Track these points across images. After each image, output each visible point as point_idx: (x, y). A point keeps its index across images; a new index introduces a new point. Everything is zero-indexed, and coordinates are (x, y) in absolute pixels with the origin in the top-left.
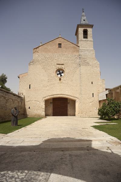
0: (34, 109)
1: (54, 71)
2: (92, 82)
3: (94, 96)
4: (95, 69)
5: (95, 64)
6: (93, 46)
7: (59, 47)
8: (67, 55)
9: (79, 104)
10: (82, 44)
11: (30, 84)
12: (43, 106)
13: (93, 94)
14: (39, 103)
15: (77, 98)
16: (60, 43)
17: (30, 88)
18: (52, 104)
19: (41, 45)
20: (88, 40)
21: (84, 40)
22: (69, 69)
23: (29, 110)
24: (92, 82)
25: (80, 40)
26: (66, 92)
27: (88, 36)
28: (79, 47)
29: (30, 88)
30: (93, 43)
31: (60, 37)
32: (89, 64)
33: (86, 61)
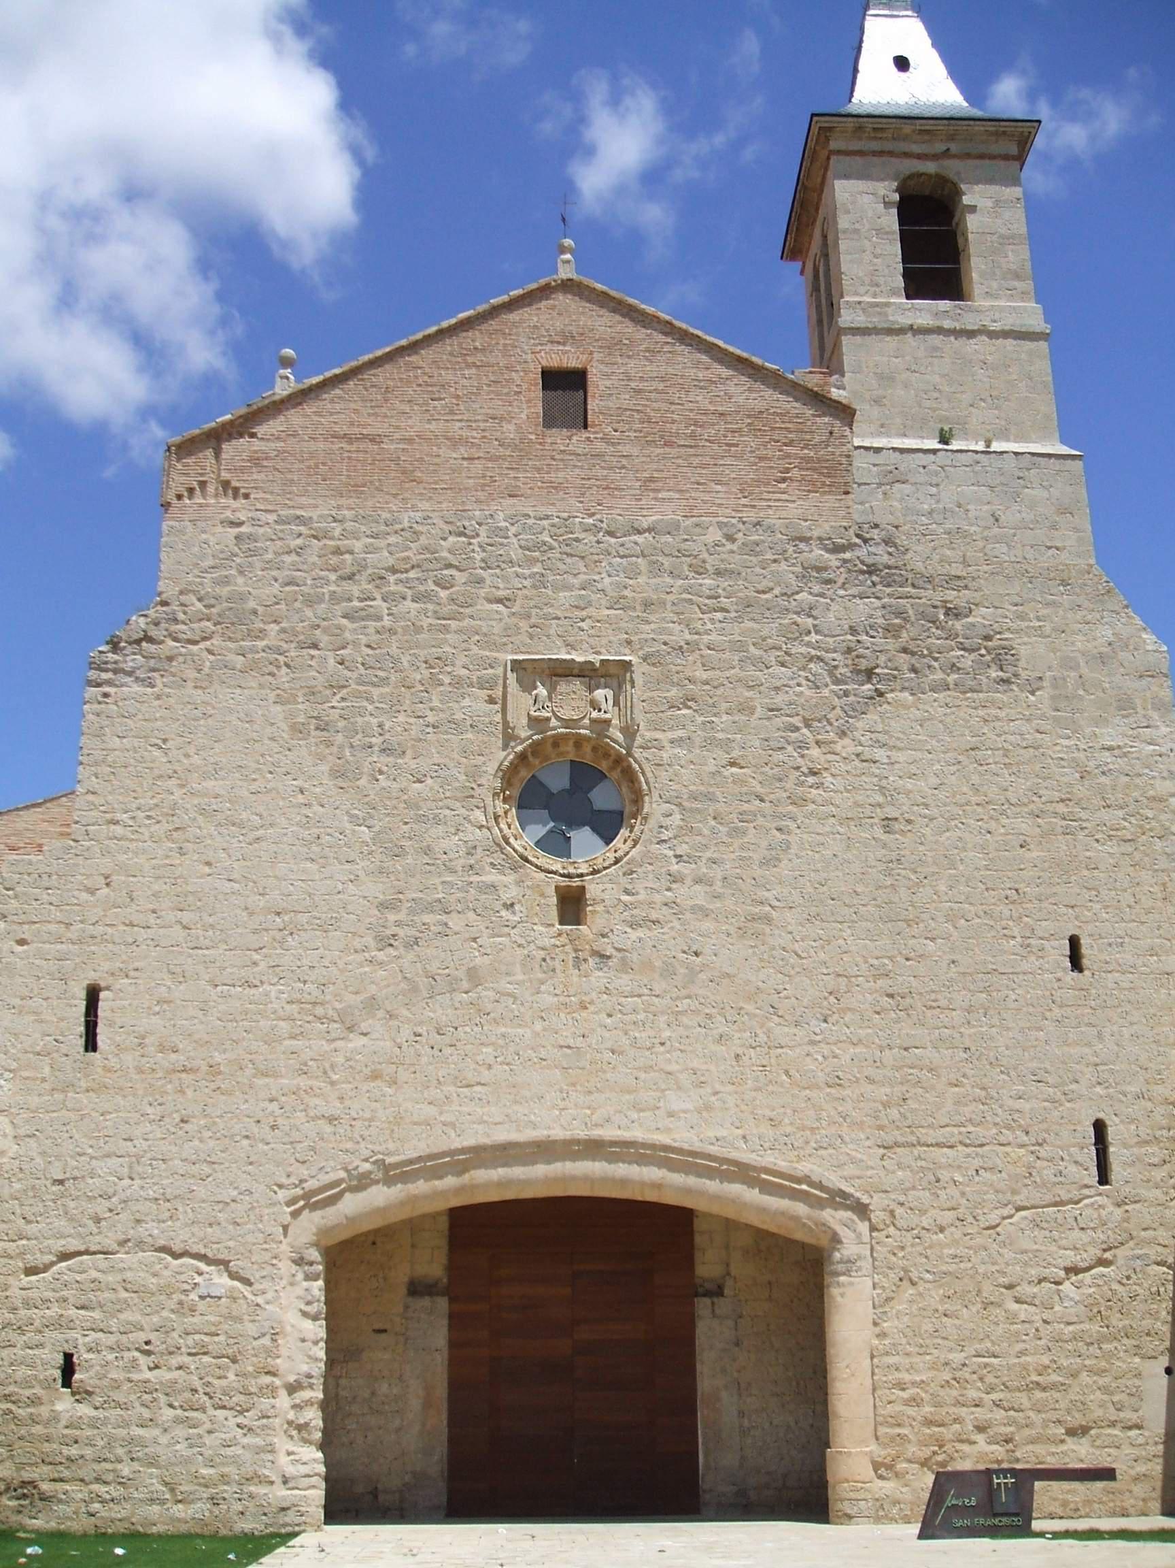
0: (146, 1388)
1: (474, 774)
2: (1074, 942)
3: (1117, 1170)
4: (1110, 735)
5: (1102, 659)
6: (1046, 406)
7: (550, 420)
8: (672, 529)
9: (882, 1304)
10: (886, 379)
11: (90, 977)
12: (287, 1345)
13: (1100, 1128)
14: (221, 1282)
15: (839, 1199)
16: (569, 359)
17: (91, 1044)
18: (443, 1303)
19: (281, 389)
20: (970, 322)
21: (924, 320)
22: (710, 743)
23: (64, 1404)
24: (1074, 942)
25: (860, 320)
26: (675, 1102)
27: (977, 267)
28: (845, 413)
29: (91, 1044)
30: (1042, 367)
31: (565, 272)
32: (1003, 657)
33: (958, 625)
